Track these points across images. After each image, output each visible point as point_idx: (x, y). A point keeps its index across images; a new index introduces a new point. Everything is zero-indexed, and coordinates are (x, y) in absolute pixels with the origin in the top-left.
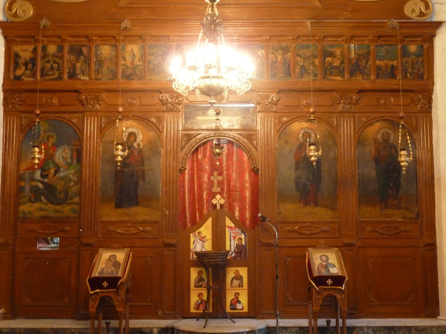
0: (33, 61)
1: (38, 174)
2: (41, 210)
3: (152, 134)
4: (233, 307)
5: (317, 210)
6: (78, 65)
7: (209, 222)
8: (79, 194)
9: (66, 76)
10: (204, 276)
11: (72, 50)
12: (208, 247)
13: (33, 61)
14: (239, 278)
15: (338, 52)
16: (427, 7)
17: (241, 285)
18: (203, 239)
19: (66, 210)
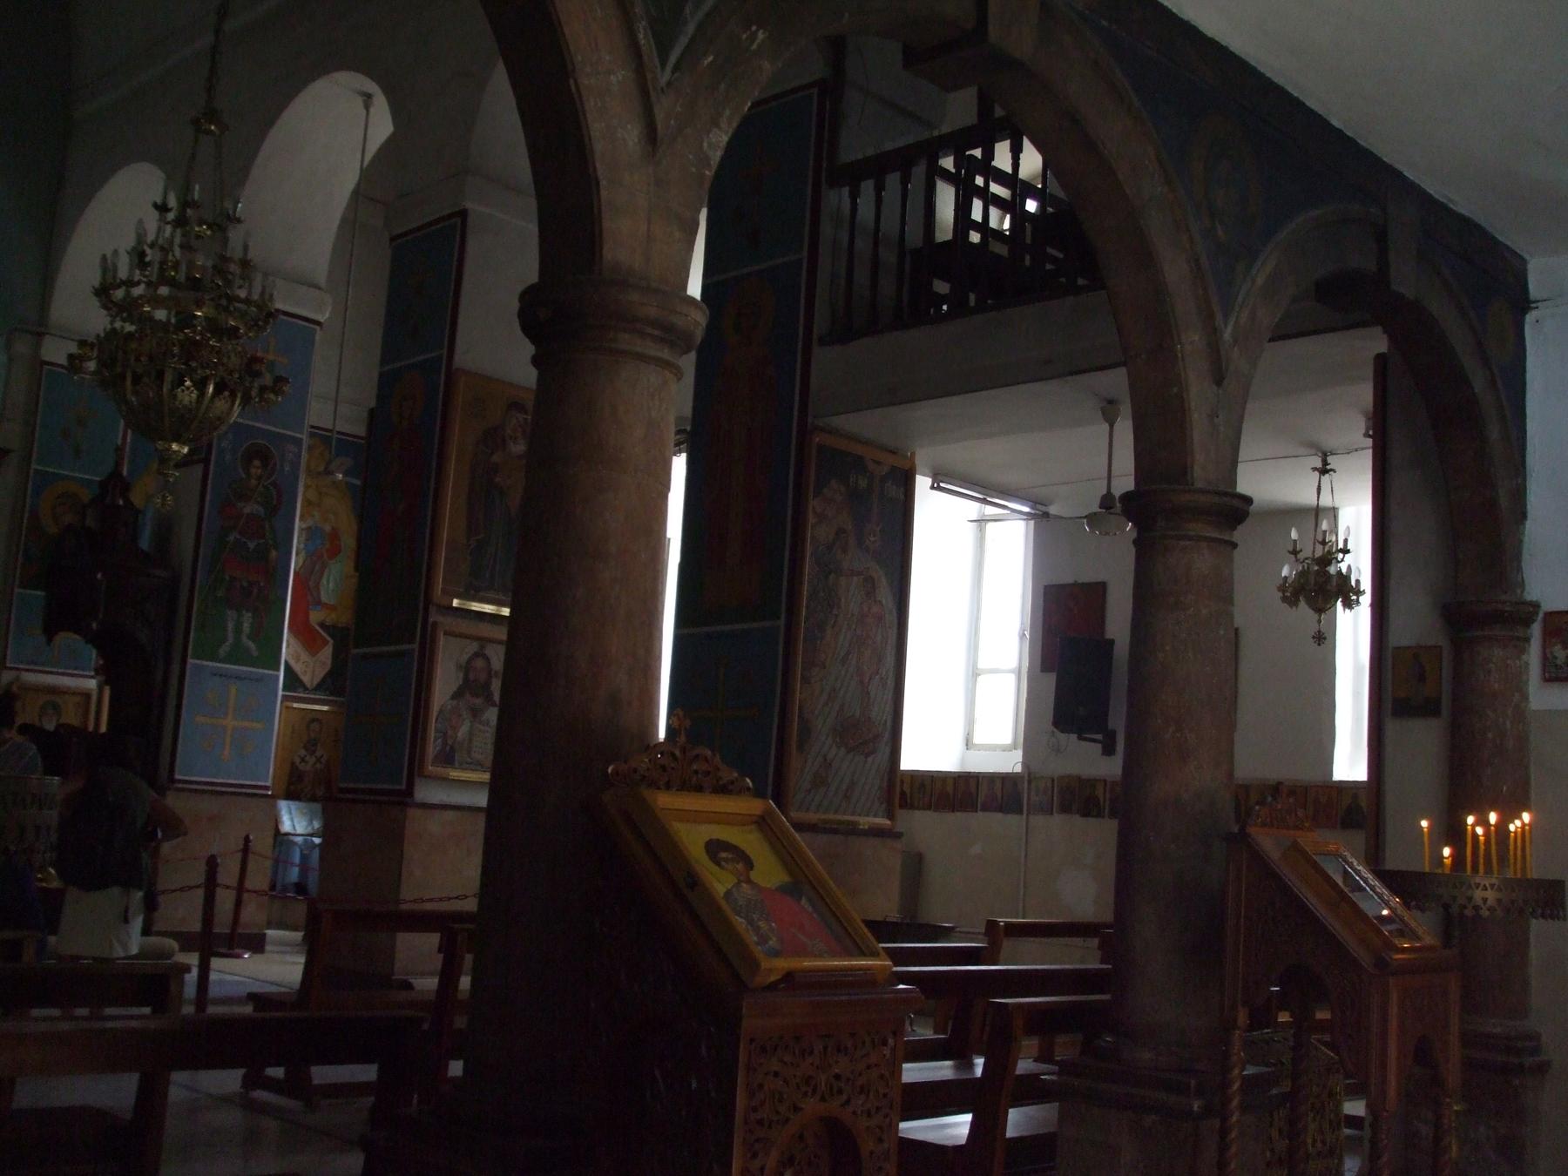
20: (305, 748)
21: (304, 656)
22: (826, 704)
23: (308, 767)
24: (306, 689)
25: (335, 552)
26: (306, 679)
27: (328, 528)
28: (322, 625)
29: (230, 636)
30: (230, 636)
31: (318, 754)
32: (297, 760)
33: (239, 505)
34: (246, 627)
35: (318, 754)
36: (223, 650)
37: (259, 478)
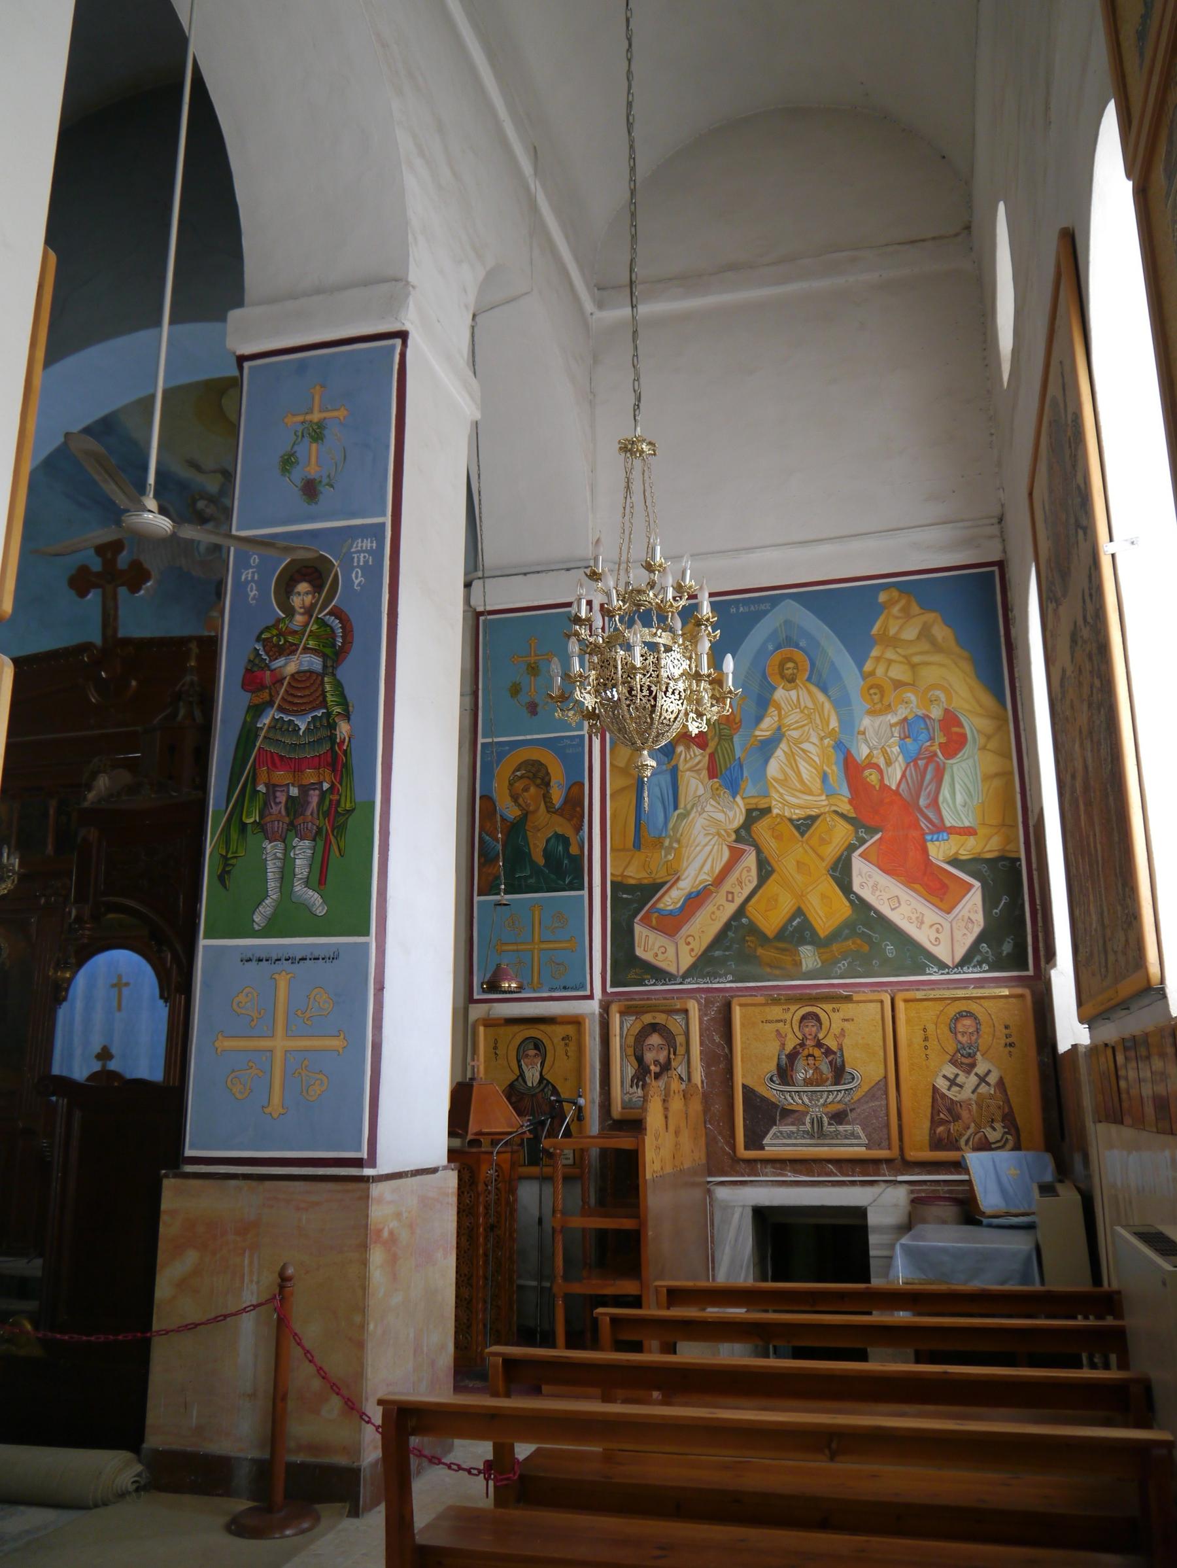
20: (953, 1062)
21: (931, 915)
23: (966, 1094)
24: (942, 966)
25: (955, 744)
26: (942, 952)
27: (936, 713)
28: (955, 862)
29: (272, 885)
30: (272, 885)
31: (981, 1069)
32: (942, 1084)
33: (280, 662)
34: (301, 865)
35: (981, 1069)
37: (309, 611)
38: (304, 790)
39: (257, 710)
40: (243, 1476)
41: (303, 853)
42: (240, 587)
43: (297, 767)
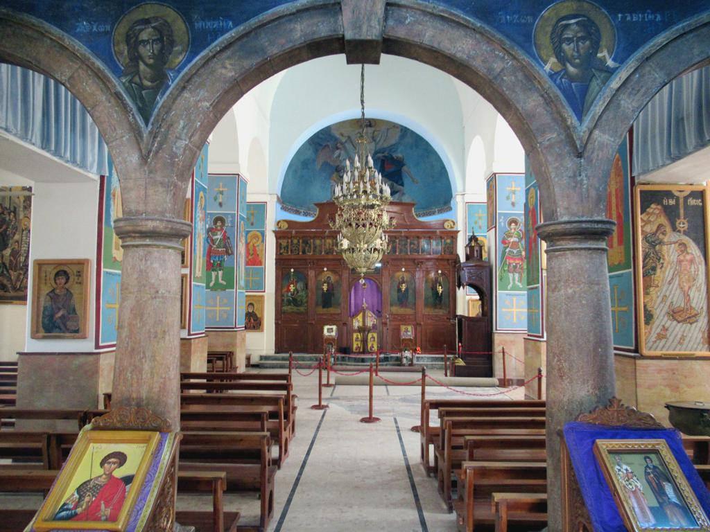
0: (287, 246)
1: (290, 294)
2: (291, 309)
3: (337, 277)
4: (371, 349)
5: (406, 309)
6: (307, 248)
7: (361, 315)
8: (307, 302)
9: (301, 253)
10: (359, 337)
11: (303, 242)
12: (361, 324)
13: (287, 246)
14: (374, 338)
15: (416, 242)
16: (454, 224)
17: (374, 340)
18: (358, 321)
19: (302, 309)
22: (661, 302)
30: (511, 281)
36: (509, 288)
38: (516, 264)
39: (506, 248)
40: (514, 382)
41: (517, 275)
42: (500, 223)
43: (515, 260)
